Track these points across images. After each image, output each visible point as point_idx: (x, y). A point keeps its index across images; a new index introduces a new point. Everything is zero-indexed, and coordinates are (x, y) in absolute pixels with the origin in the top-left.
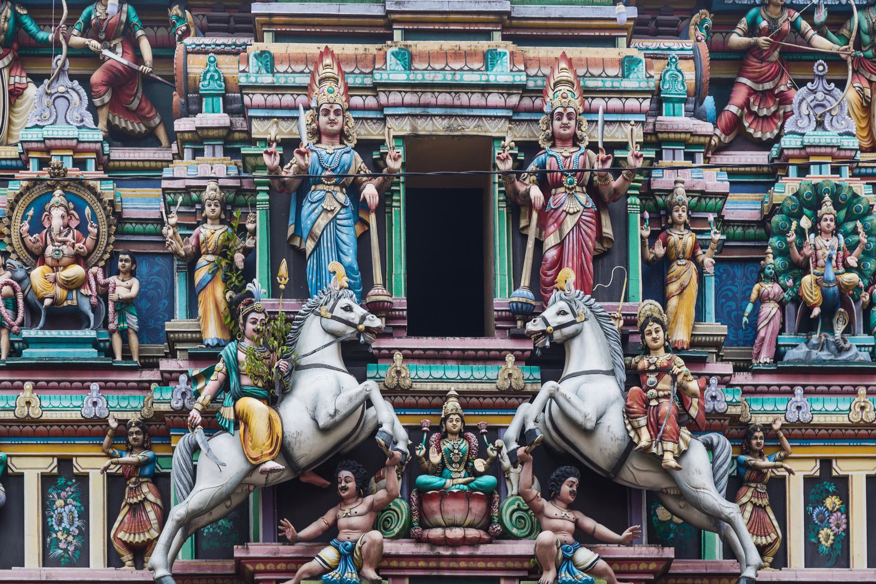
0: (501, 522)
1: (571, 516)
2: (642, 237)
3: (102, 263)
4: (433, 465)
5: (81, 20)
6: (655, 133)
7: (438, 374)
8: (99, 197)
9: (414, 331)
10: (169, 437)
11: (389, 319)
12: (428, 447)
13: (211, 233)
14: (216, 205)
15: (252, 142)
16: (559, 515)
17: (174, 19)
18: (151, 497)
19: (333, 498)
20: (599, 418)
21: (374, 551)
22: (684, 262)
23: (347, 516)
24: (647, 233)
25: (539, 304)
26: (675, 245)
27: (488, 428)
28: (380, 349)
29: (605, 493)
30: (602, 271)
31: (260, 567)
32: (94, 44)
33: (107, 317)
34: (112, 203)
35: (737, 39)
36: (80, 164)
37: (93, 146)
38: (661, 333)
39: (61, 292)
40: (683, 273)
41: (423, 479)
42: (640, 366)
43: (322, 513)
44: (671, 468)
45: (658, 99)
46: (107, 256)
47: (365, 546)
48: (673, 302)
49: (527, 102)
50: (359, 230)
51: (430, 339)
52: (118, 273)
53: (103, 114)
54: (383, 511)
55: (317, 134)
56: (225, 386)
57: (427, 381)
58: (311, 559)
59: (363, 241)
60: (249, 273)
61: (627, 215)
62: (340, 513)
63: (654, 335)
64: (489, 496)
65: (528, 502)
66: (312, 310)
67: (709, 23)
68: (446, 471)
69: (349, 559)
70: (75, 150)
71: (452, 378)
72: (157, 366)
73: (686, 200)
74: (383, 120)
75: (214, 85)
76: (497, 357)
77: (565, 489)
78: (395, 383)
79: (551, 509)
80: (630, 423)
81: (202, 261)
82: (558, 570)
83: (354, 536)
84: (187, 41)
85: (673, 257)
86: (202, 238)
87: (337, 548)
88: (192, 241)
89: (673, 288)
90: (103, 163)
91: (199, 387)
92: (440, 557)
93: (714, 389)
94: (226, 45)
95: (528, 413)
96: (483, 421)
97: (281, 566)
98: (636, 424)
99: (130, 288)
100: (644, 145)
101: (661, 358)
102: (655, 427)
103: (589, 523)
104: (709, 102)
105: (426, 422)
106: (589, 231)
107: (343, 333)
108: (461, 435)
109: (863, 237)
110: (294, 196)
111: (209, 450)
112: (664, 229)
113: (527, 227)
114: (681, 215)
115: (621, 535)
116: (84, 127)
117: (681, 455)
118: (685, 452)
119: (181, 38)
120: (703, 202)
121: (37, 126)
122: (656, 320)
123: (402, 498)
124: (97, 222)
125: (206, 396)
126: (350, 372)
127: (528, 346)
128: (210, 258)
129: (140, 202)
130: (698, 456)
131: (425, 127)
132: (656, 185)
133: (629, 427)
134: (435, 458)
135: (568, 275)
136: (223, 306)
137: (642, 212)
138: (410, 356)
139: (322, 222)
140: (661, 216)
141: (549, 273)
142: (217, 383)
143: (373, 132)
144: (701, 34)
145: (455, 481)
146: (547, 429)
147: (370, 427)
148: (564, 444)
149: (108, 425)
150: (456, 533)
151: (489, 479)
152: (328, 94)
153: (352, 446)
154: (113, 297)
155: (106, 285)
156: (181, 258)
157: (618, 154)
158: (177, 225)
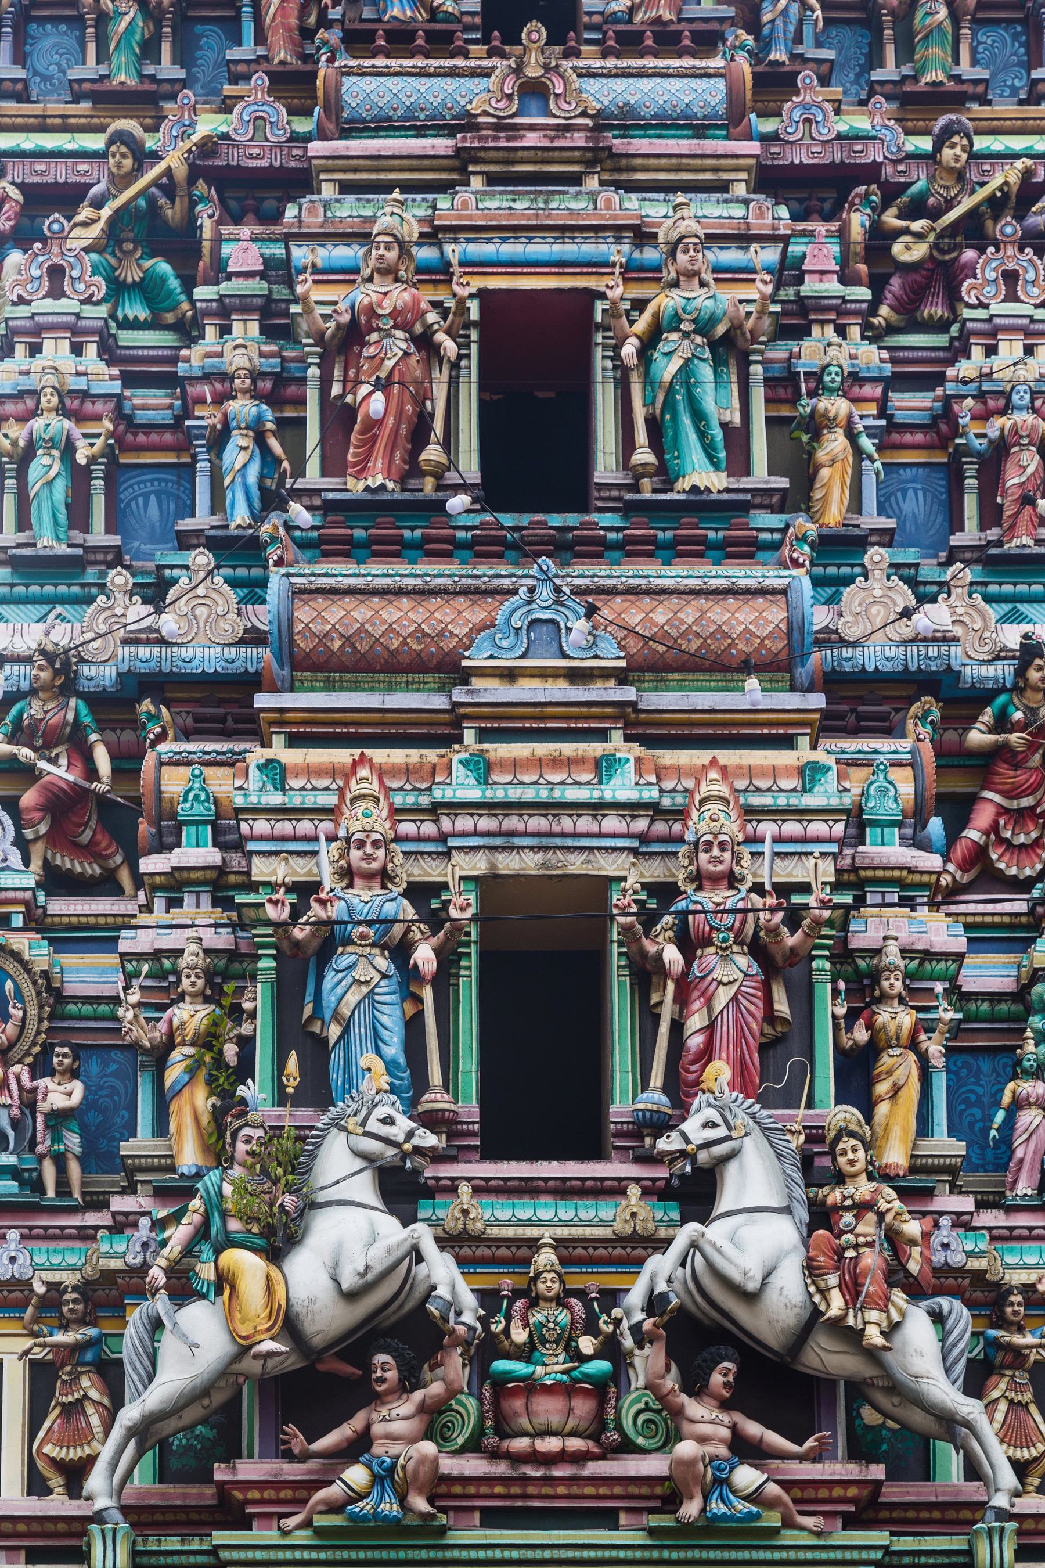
0: (619, 1427)
1: (726, 1418)
2: (834, 1016)
3: (29, 1060)
4: (517, 1346)
5: (7, 720)
6: (854, 869)
7: (524, 1212)
8: (26, 966)
9: (490, 1153)
10: (123, 1307)
11: (451, 1136)
12: (509, 1318)
13: (191, 1015)
14: (198, 976)
15: (252, 887)
16: (707, 1418)
17: (143, 718)
18: (94, 1394)
19: (365, 1394)
20: (767, 1275)
21: (424, 1470)
22: (898, 1051)
23: (384, 1420)
24: (841, 1011)
25: (677, 1112)
26: (884, 1027)
27: (601, 1292)
28: (438, 1179)
29: (779, 1385)
30: (774, 1065)
31: (254, 1494)
32: (25, 753)
34: (45, 974)
37: (20, 895)
38: (861, 1154)
40: (899, 1067)
41: (501, 1365)
42: (830, 1201)
43: (348, 1416)
44: (876, 1347)
45: (858, 822)
46: (37, 1049)
47: (411, 1463)
48: (883, 1109)
49: (660, 827)
50: (410, 1009)
51: (514, 1163)
52: (52, 1073)
53: (37, 852)
54: (441, 1413)
56: (202, 1233)
57: (508, 1223)
58: (331, 1483)
60: (245, 1070)
61: (810, 986)
62: (374, 1416)
63: (851, 1156)
64: (601, 1390)
65: (661, 1398)
67: (936, 714)
68: (536, 1354)
71: (547, 1219)
72: (107, 1205)
73: (901, 963)
74: (447, 854)
75: (199, 808)
76: (615, 1189)
77: (717, 1379)
78: (460, 1226)
79: (695, 1408)
80: (814, 1282)
81: (176, 1055)
82: (706, 1498)
83: (395, 1449)
84: (162, 747)
85: (882, 1044)
86: (176, 1022)
87: (369, 1467)
88: (162, 1026)
90: (37, 921)
91: (166, 1235)
92: (526, 1480)
93: (945, 1233)
94: (218, 753)
95: (660, 1269)
96: (593, 1281)
97: (286, 1494)
98: (822, 1284)
99: (70, 1094)
100: (837, 887)
101: (862, 1188)
102: (852, 1289)
103: (753, 1429)
104: (936, 826)
105: (507, 1284)
106: (752, 1008)
107: (381, 1157)
108: (560, 1301)
110: (313, 961)
111: (175, 1324)
112: (868, 1005)
114: (894, 984)
115: (801, 1444)
116: (8, 868)
117: (892, 1330)
118: (898, 1325)
119: (154, 744)
120: (928, 966)
122: (852, 1134)
123: (471, 1394)
124: (23, 1002)
126: (392, 1212)
128: (188, 1050)
129: (87, 974)
131: (509, 864)
132: (855, 943)
133: (812, 1289)
134: (519, 1335)
135: (720, 1072)
137: (834, 981)
138: (483, 1188)
139: (353, 998)
140: (863, 985)
141: (693, 1068)
142: (191, 1228)
144: (924, 731)
145: (549, 1369)
146: (690, 1293)
147: (420, 1290)
148: (714, 1314)
149: (32, 1290)
150: (551, 1444)
151: (601, 1366)
152: (366, 819)
153: (394, 1319)
154: (43, 1107)
155: (34, 1090)
156: (146, 1052)
157: (797, 899)
158: (139, 1005)
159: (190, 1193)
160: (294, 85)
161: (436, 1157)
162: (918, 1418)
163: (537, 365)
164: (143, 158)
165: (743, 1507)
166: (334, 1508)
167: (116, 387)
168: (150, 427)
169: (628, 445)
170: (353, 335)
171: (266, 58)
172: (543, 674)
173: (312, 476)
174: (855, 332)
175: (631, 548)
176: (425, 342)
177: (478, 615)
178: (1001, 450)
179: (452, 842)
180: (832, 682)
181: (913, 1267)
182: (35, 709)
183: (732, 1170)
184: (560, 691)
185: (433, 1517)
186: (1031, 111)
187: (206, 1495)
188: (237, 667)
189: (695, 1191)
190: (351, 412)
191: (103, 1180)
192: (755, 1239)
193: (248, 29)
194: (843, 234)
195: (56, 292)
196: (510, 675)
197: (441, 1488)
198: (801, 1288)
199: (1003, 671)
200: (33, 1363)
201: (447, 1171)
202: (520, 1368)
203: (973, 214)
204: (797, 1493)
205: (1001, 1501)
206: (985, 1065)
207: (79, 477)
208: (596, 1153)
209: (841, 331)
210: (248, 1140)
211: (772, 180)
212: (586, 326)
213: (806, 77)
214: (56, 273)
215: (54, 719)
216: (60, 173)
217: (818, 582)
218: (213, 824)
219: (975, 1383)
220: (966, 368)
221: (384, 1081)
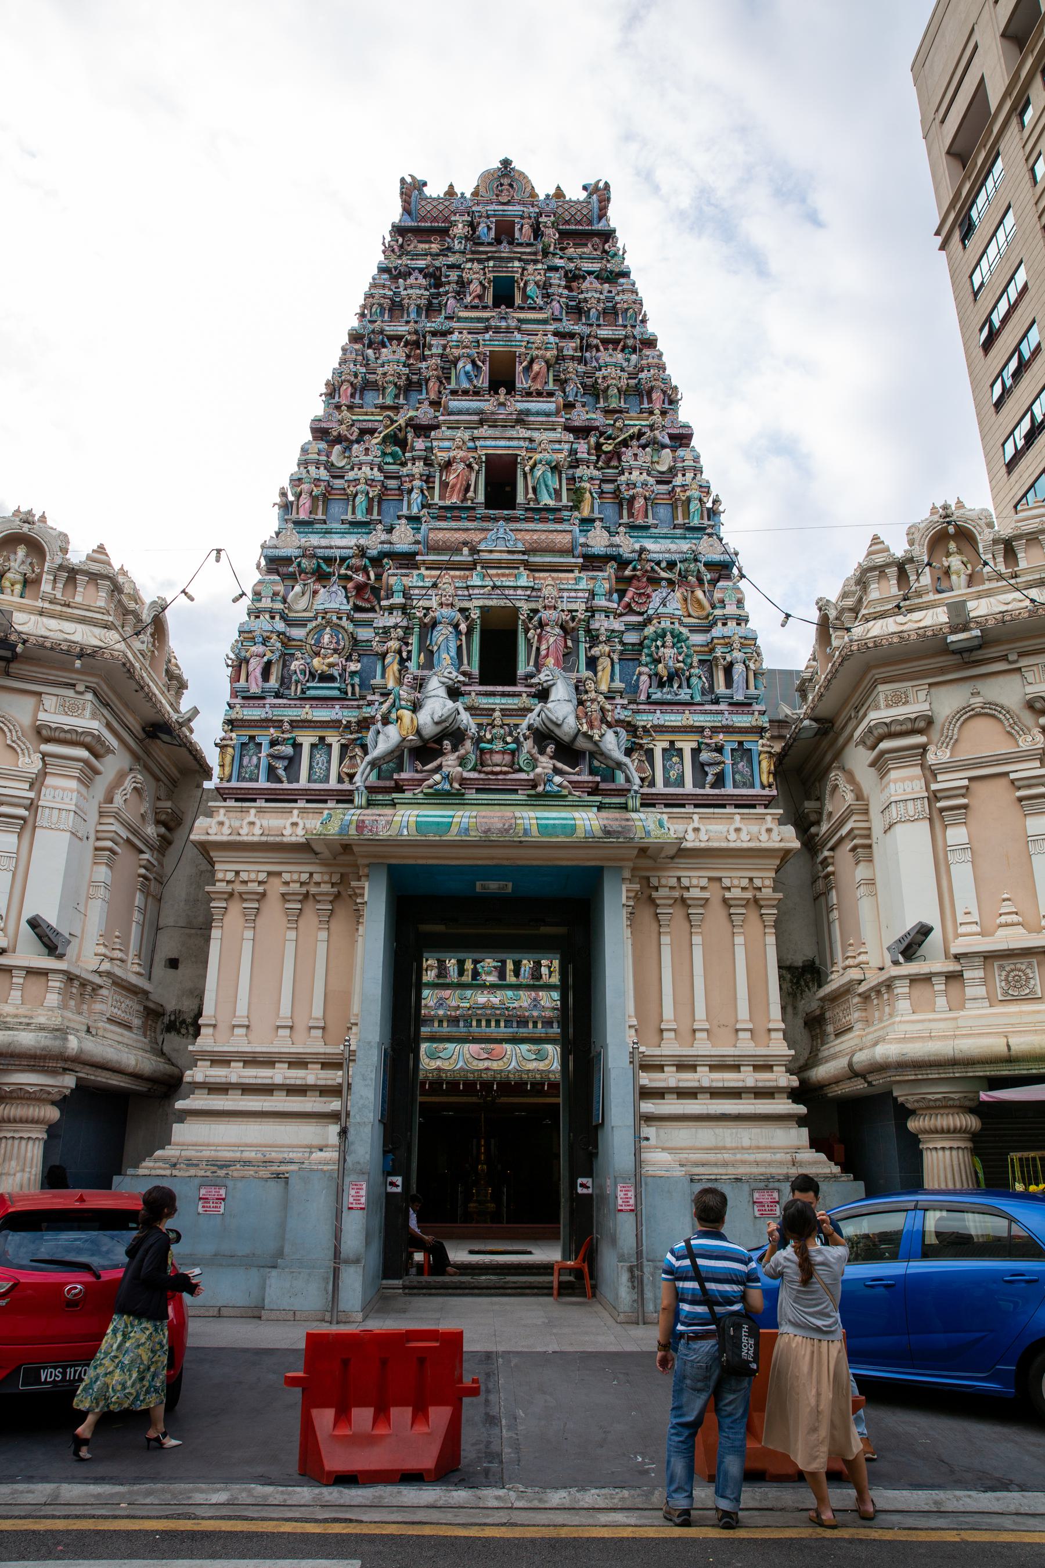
9: (481, 684)
13: (394, 644)
19: (441, 753)
21: (458, 776)
24: (588, 646)
29: (568, 752)
32: (349, 573)
36: (340, 618)
39: (325, 668)
40: (604, 663)
41: (483, 745)
48: (600, 674)
53: (352, 600)
56: (393, 705)
59: (459, 648)
60: (409, 659)
66: (435, 674)
76: (518, 695)
77: (548, 750)
83: (449, 769)
89: (600, 668)
95: (531, 718)
100: (586, 611)
103: (559, 765)
104: (615, 596)
108: (501, 727)
109: (685, 649)
114: (603, 638)
117: (602, 736)
127: (533, 690)
129: (364, 634)
136: (397, 675)
140: (594, 639)
143: (466, 604)
144: (612, 571)
150: (498, 769)
151: (514, 746)
154: (348, 670)
159: (389, 694)
160: (435, 404)
161: (465, 684)
162: (611, 763)
163: (501, 483)
164: (393, 422)
165: (556, 788)
166: (430, 787)
168: (391, 489)
169: (527, 493)
170: (448, 464)
172: (501, 551)
173: (436, 500)
174: (592, 467)
175: (526, 520)
176: (469, 466)
177: (482, 536)
178: (633, 498)
180: (585, 556)
181: (609, 719)
182: (353, 561)
184: (505, 556)
187: (392, 784)
188: (412, 550)
189: (543, 695)
190: (448, 483)
191: (364, 692)
192: (561, 707)
193: (424, 391)
194: (588, 443)
195: (367, 454)
196: (491, 551)
197: (463, 781)
199: (635, 556)
200: (342, 745)
201: (468, 688)
202: (489, 746)
203: (625, 440)
205: (636, 788)
206: (631, 663)
207: (370, 501)
208: (514, 684)
209: (588, 467)
211: (568, 429)
212: (515, 463)
213: (578, 405)
214: (367, 449)
215: (359, 564)
216: (370, 425)
217: (581, 531)
219: (628, 752)
220: (623, 478)
221: (449, 662)
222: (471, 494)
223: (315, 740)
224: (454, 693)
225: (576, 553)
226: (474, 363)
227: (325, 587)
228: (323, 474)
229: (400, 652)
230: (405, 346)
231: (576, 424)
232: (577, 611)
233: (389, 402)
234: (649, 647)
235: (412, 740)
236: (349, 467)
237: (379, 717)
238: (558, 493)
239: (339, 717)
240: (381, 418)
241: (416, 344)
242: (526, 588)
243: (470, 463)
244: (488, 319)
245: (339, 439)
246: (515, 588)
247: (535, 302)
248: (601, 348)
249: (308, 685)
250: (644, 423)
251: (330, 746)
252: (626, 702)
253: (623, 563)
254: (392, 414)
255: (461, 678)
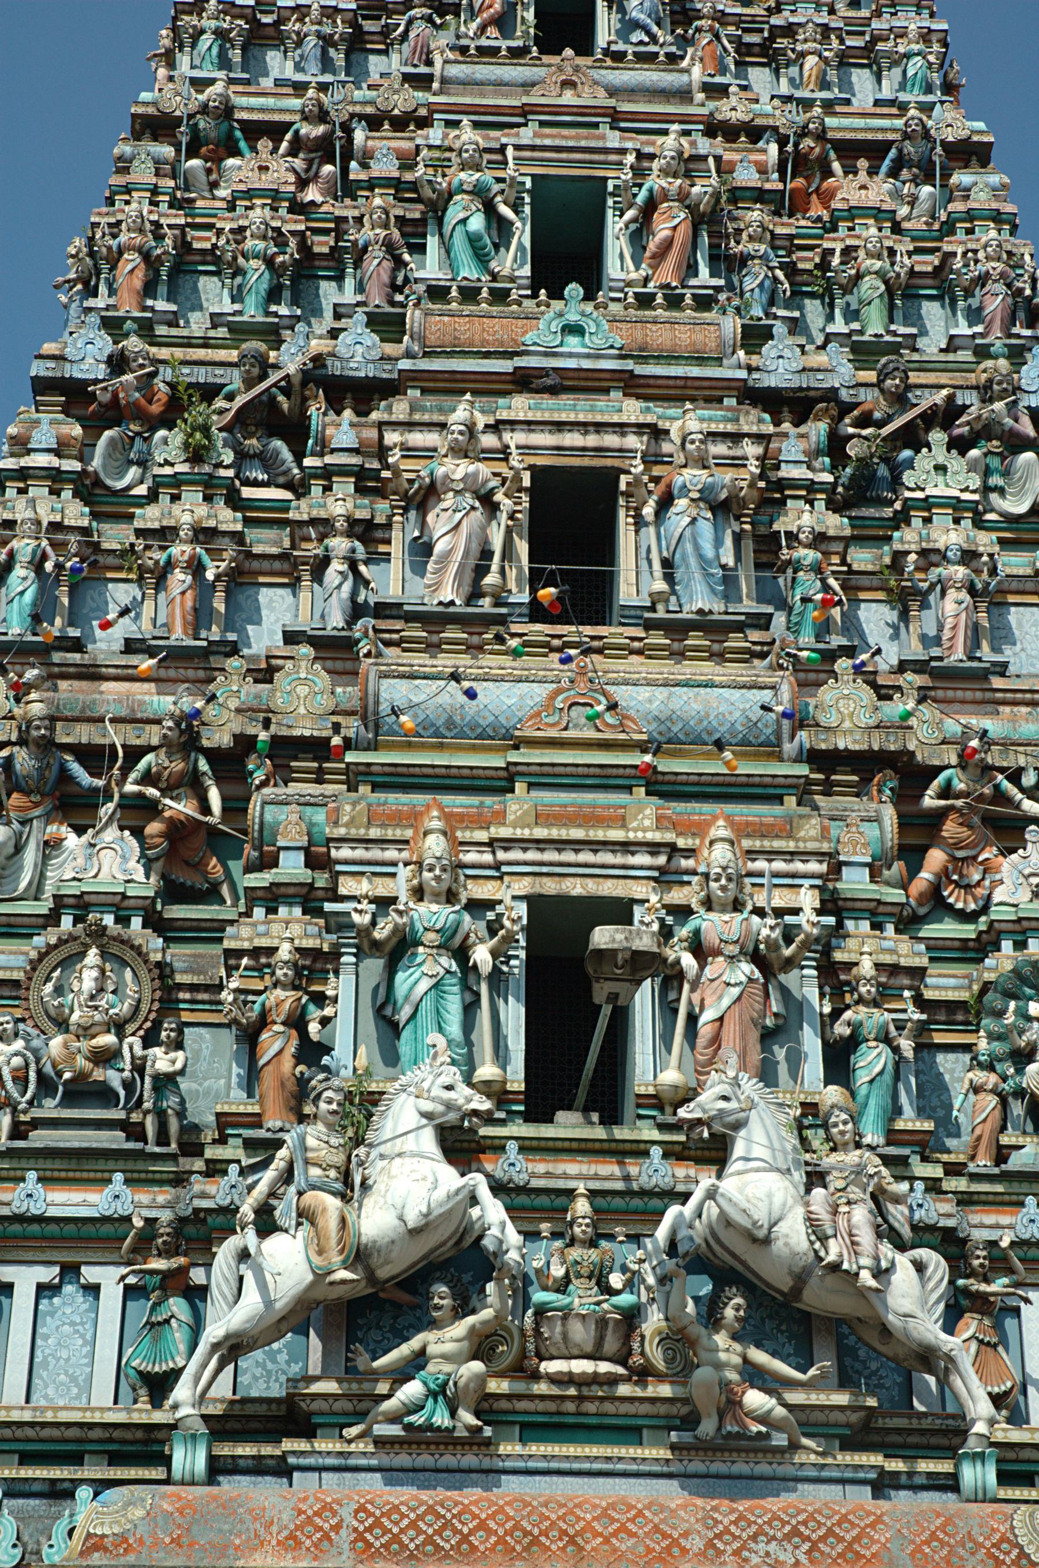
0: (643, 1354)
1: (738, 1347)
3: (141, 1033)
4: (555, 1280)
24: (827, 1009)
32: (152, 792)
33: (141, 1095)
34: (159, 965)
35: (929, 801)
36: (123, 920)
46: (148, 1024)
47: (463, 1380)
55: (419, 893)
56: (288, 1176)
68: (571, 1287)
69: (440, 1398)
70: (118, 908)
76: (639, 1150)
77: (729, 1313)
83: (448, 1368)
84: (266, 791)
88: (257, 1007)
89: (862, 1078)
90: (155, 922)
99: (173, 1062)
103: (759, 1356)
104: (898, 868)
113: (678, 1000)
117: (881, 1273)
119: (259, 788)
121: (74, 879)
125: (262, 1188)
130: (904, 1274)
132: (838, 956)
137: (821, 987)
148: (727, 1258)
151: (626, 1299)
155: (144, 1058)
157: (789, 919)
161: (488, 1119)
164: (265, 367)
166: (394, 1418)
167: (239, 527)
171: (363, 304)
179: (504, 869)
183: (743, 1133)
185: (479, 1429)
186: (951, 357)
198: (804, 1237)
203: (909, 425)
204: (803, 1417)
210: (330, 1102)
213: (779, 329)
216: (201, 375)
218: (307, 850)
222: (491, 579)
223: (48, 1274)
224: (460, 1144)
225: (789, 748)
226: (489, 209)
227: (80, 830)
228: (75, 513)
229: (297, 1022)
230: (293, 152)
231: (771, 381)
232: (796, 911)
233: (251, 311)
234: (1000, 1014)
235: (344, 1282)
236: (142, 490)
237: (247, 1210)
238: (729, 579)
239: (122, 1208)
240: (233, 355)
241: (323, 150)
242: (653, 848)
243: (492, 492)
244: (528, 86)
245: (114, 413)
246: (627, 847)
247: (654, 39)
248: (836, 166)
249: (36, 1113)
250: (958, 378)
251: (93, 1290)
252: (938, 1172)
253: (911, 774)
254: (262, 347)
255: (482, 1104)
